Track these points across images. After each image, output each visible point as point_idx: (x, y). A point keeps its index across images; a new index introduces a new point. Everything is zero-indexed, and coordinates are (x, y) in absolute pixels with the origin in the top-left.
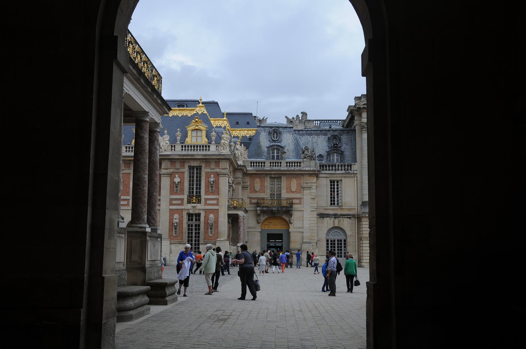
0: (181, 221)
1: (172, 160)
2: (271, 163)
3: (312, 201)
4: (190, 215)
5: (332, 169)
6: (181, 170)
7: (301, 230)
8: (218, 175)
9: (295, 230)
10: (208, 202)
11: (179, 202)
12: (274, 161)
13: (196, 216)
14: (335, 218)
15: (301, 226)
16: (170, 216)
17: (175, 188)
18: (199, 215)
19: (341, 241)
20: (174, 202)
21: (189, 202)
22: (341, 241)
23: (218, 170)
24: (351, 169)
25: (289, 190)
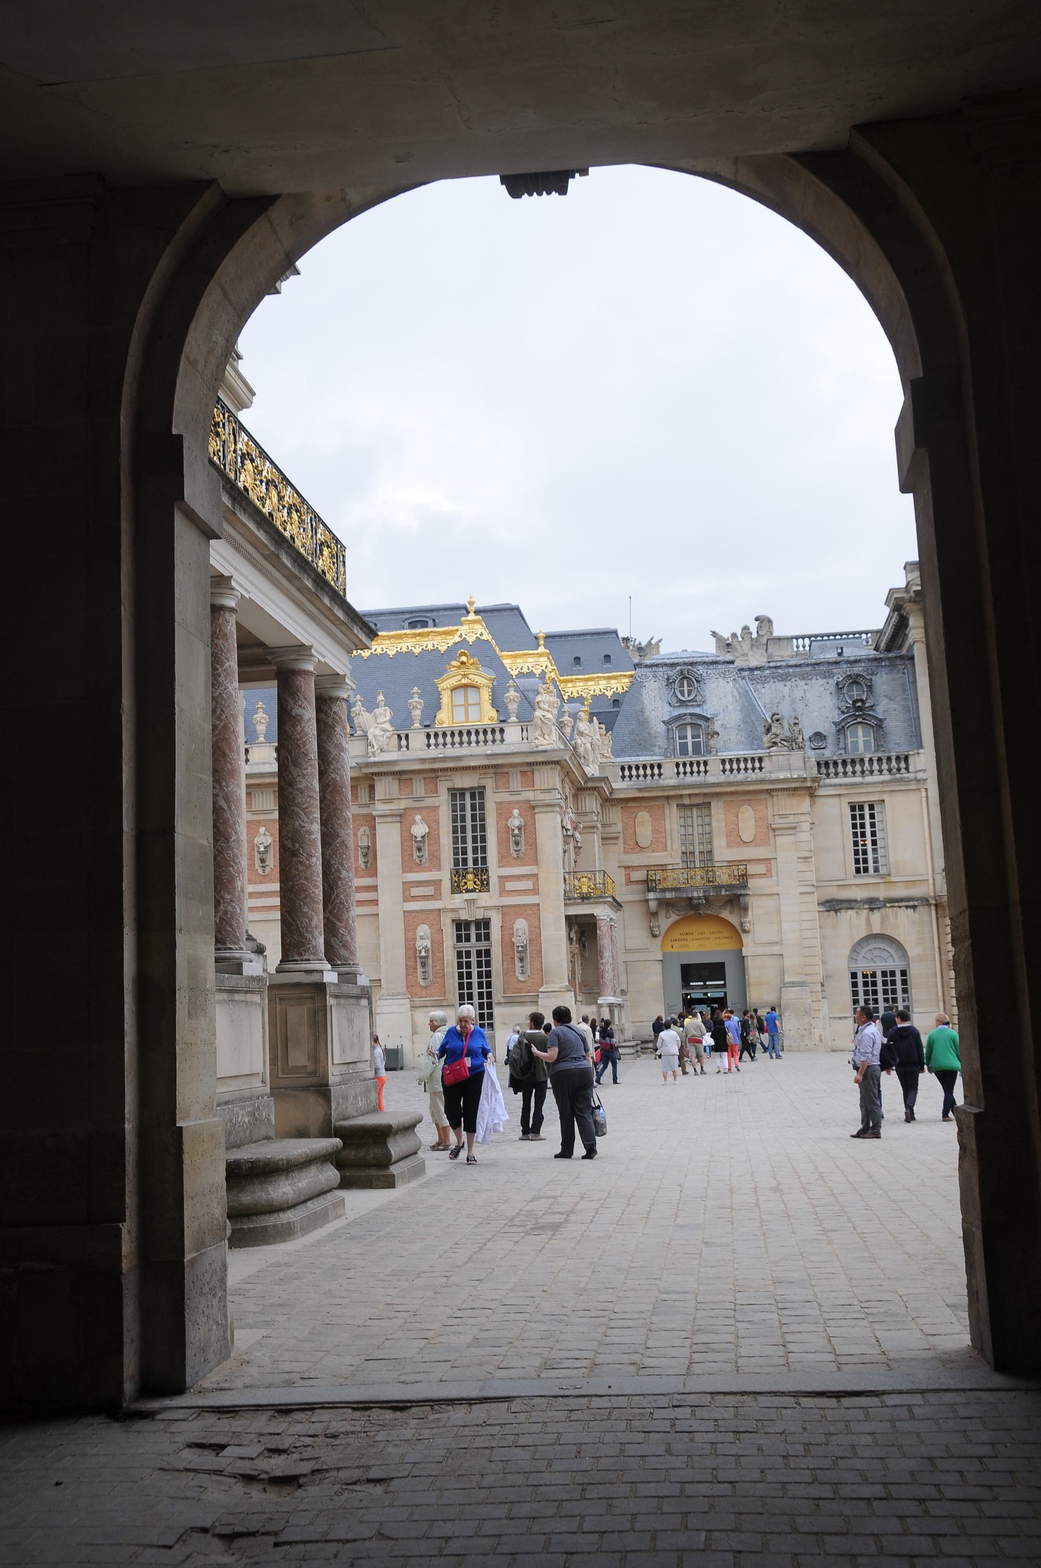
0: (438, 944)
1: (402, 776)
2: (677, 765)
3: (802, 867)
4: (461, 926)
5: (854, 773)
6: (429, 802)
7: (776, 950)
8: (531, 808)
9: (760, 950)
10: (510, 886)
11: (429, 890)
12: (687, 760)
13: (478, 928)
14: (872, 909)
15: (775, 939)
16: (406, 931)
17: (415, 852)
18: (486, 923)
19: (893, 973)
20: (415, 891)
21: (456, 889)
22: (893, 973)
23: (530, 795)
24: (907, 769)
25: (735, 839)
